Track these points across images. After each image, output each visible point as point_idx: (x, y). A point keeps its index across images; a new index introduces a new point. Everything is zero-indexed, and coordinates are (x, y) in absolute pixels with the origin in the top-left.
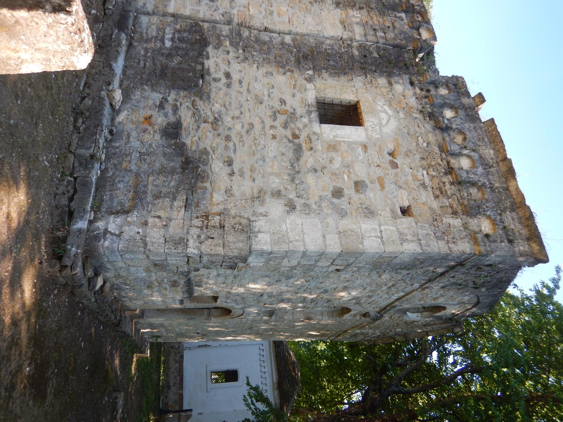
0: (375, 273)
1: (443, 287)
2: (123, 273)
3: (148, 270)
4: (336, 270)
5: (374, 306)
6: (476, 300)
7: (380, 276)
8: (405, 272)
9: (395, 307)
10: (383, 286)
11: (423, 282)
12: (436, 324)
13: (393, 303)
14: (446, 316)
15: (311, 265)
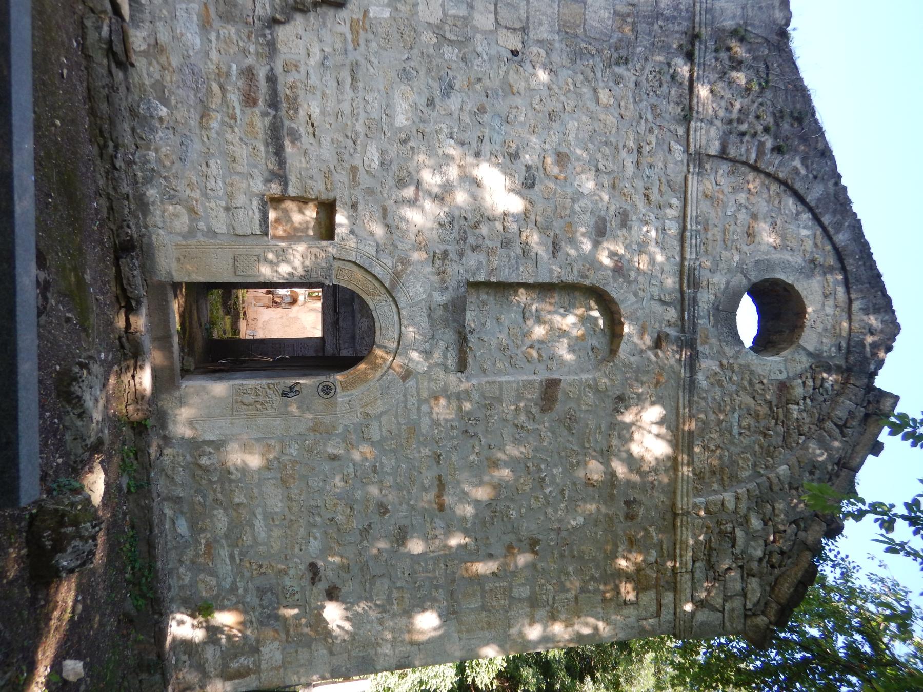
0: (582, 78)
1: (723, 155)
2: (164, 37)
3: (205, 25)
4: (515, 53)
5: (657, 297)
6: (829, 247)
7: (595, 90)
8: (628, 74)
9: (695, 284)
10: (624, 154)
11: (681, 131)
12: (834, 402)
13: (683, 258)
14: (831, 358)
15: (466, 20)
